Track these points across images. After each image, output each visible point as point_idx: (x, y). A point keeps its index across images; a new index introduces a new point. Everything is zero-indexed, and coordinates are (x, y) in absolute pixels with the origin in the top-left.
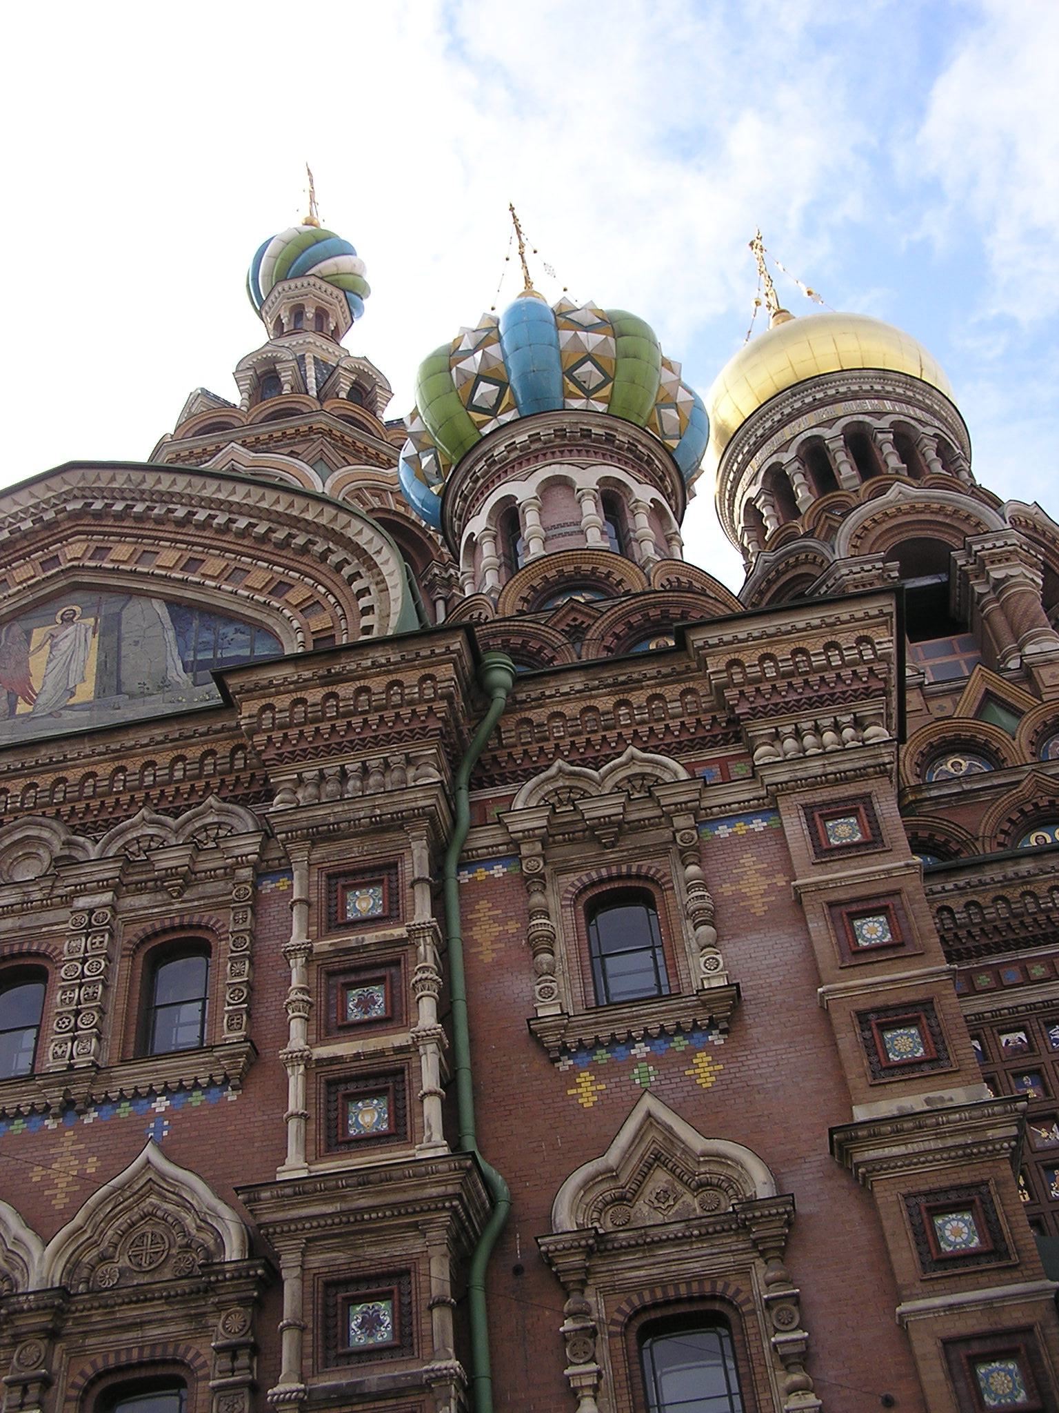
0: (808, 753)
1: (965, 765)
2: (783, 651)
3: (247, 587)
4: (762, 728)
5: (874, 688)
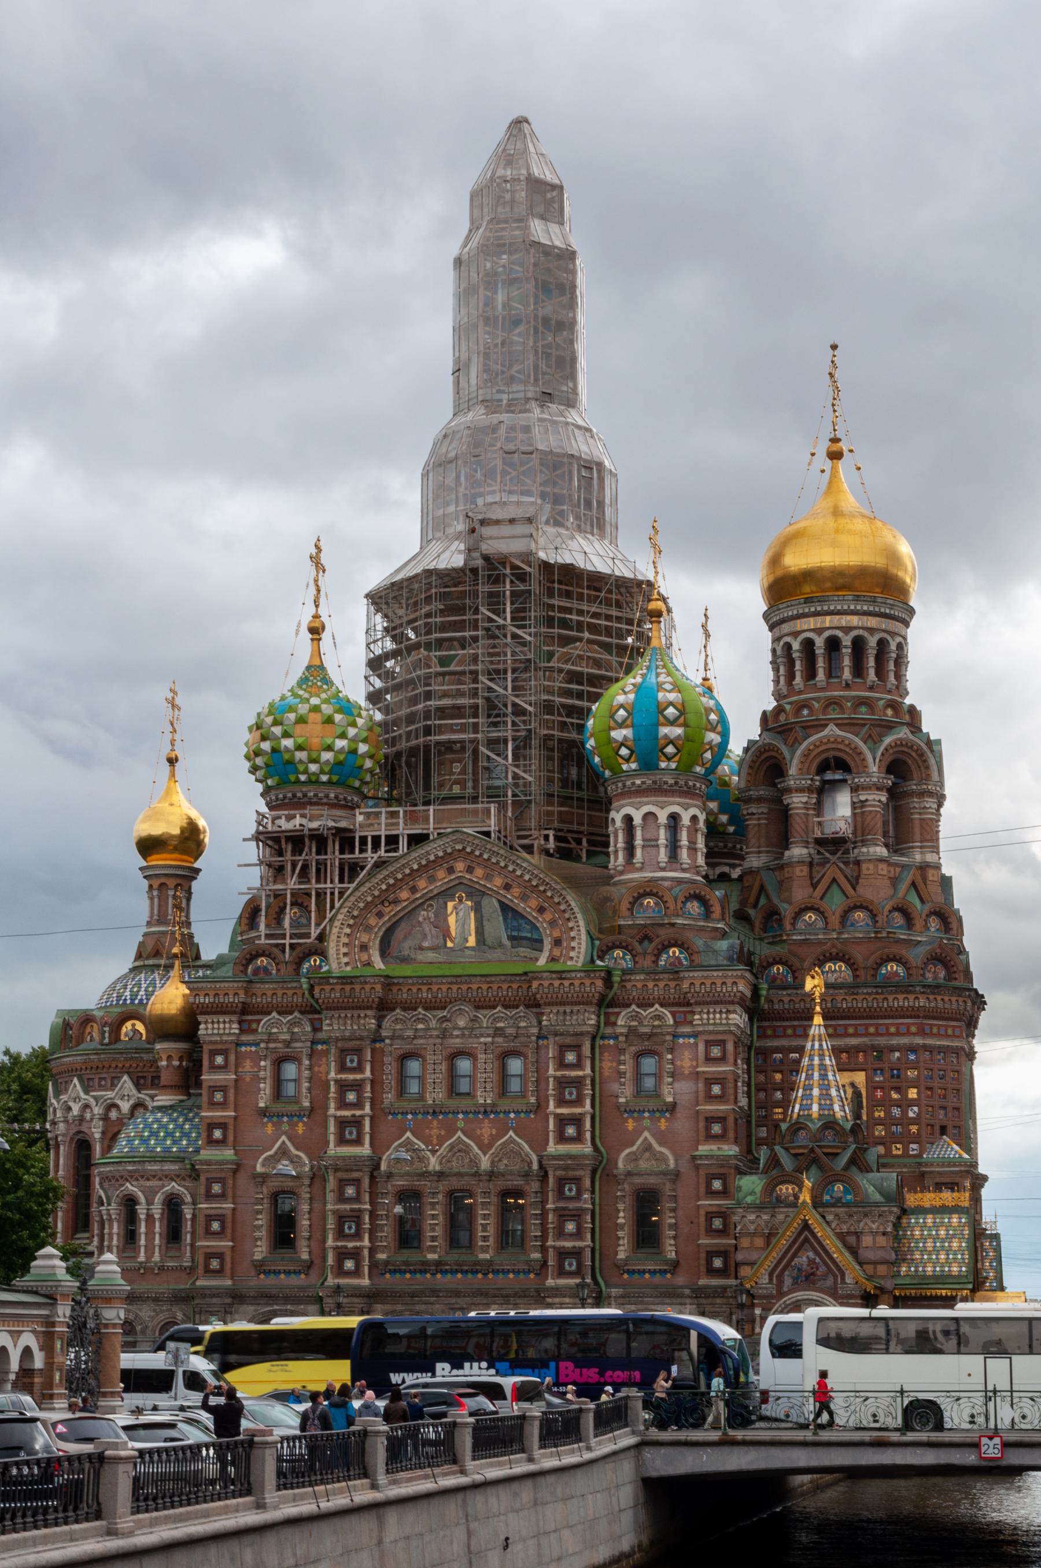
1: (814, 918)
2: (708, 982)
3: (530, 907)
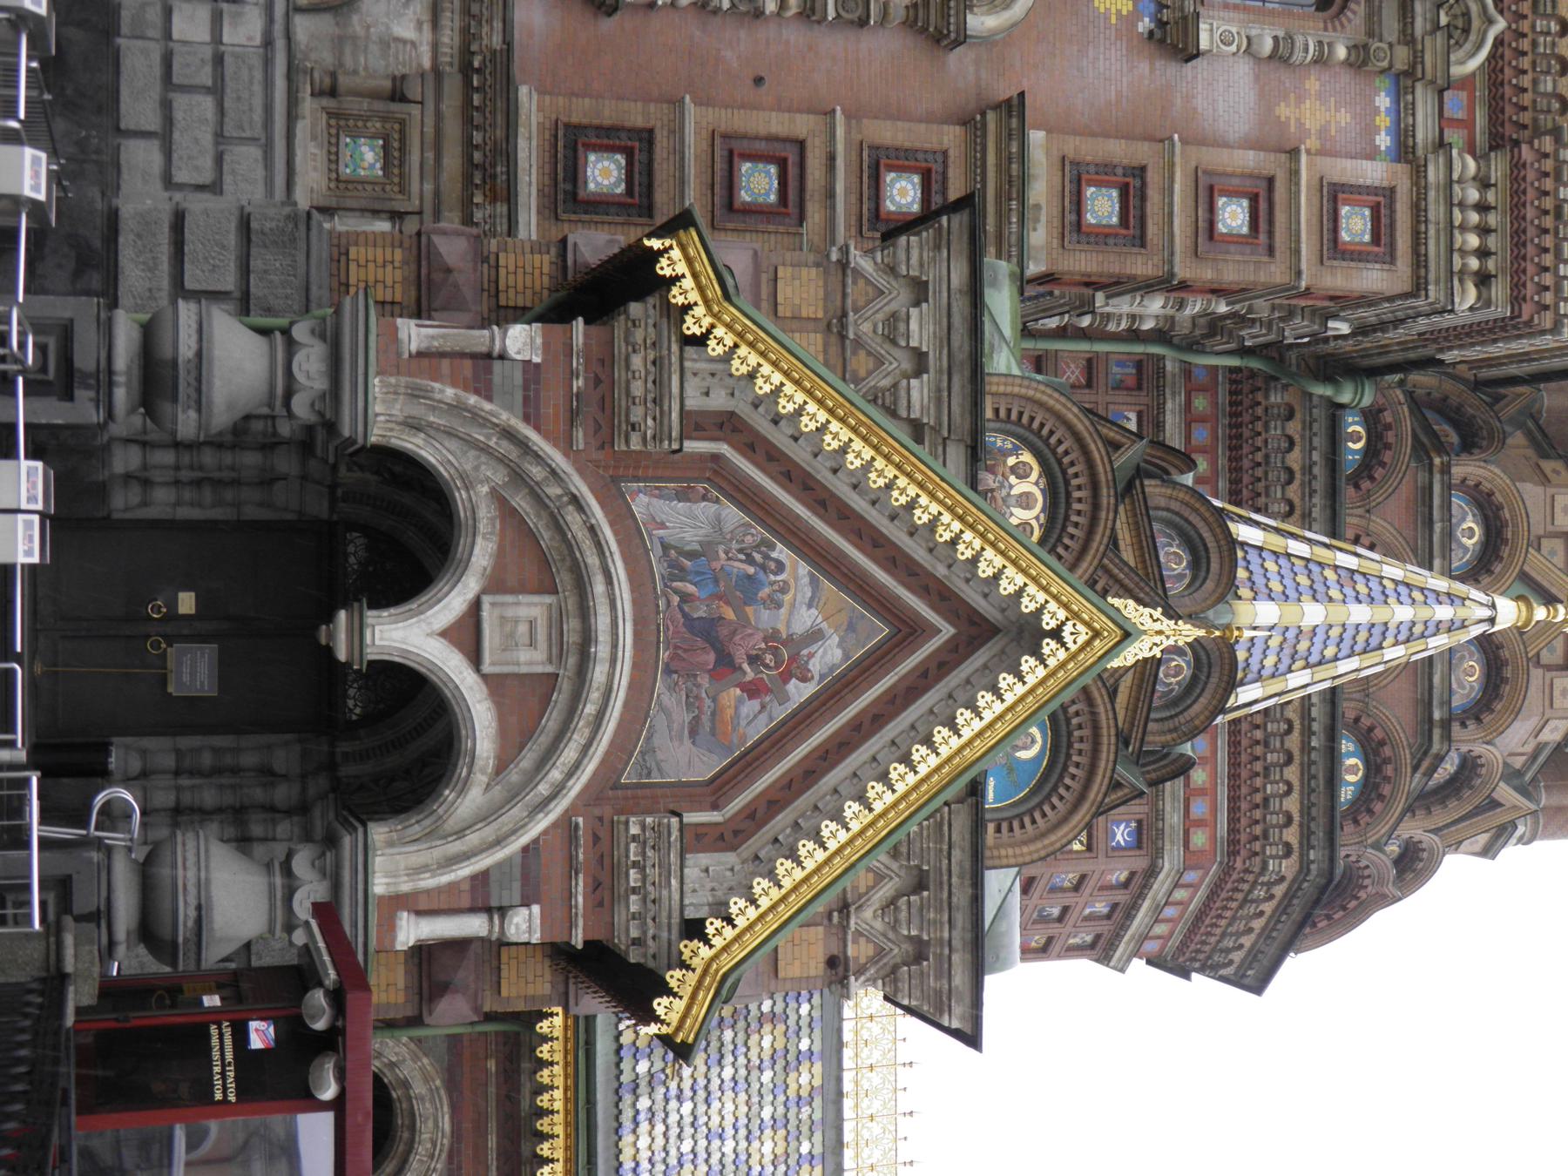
0: (1456, 212)
1: (1469, 543)
4: (1498, 168)
5: (1524, 306)
